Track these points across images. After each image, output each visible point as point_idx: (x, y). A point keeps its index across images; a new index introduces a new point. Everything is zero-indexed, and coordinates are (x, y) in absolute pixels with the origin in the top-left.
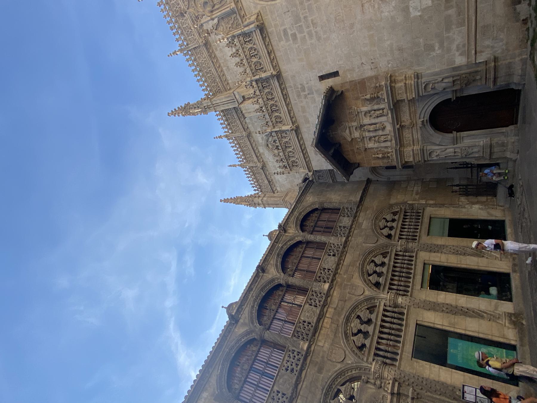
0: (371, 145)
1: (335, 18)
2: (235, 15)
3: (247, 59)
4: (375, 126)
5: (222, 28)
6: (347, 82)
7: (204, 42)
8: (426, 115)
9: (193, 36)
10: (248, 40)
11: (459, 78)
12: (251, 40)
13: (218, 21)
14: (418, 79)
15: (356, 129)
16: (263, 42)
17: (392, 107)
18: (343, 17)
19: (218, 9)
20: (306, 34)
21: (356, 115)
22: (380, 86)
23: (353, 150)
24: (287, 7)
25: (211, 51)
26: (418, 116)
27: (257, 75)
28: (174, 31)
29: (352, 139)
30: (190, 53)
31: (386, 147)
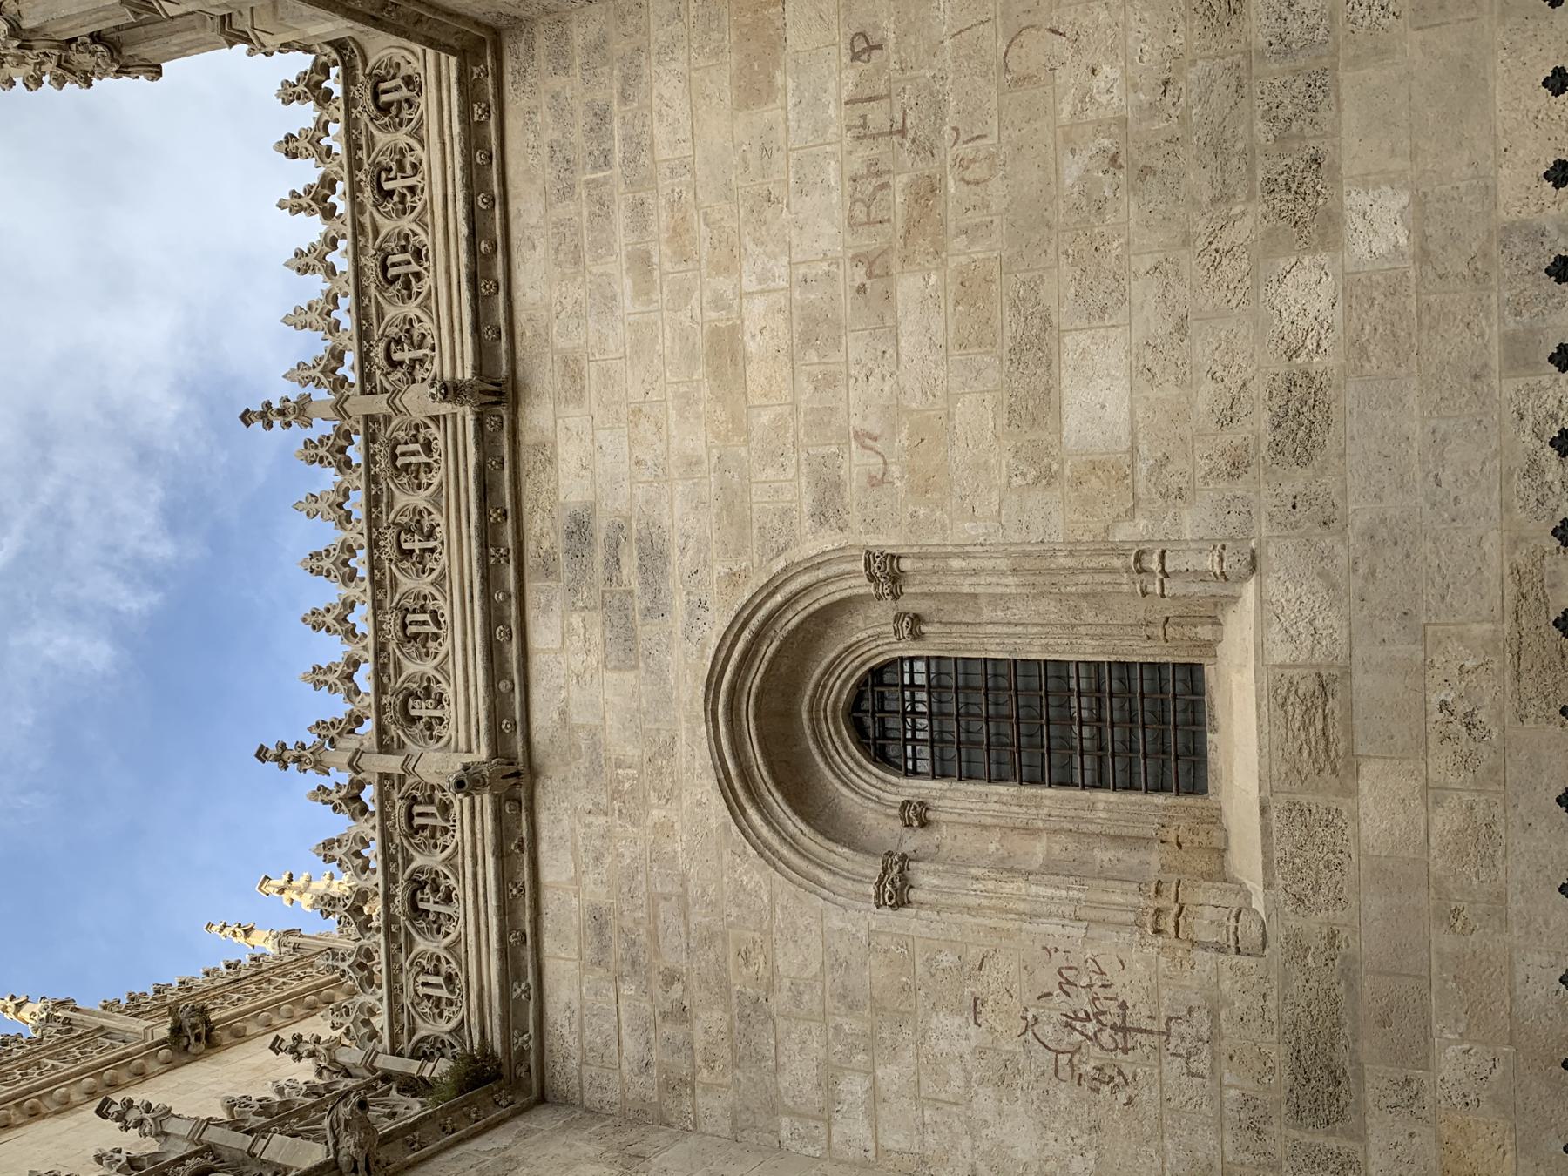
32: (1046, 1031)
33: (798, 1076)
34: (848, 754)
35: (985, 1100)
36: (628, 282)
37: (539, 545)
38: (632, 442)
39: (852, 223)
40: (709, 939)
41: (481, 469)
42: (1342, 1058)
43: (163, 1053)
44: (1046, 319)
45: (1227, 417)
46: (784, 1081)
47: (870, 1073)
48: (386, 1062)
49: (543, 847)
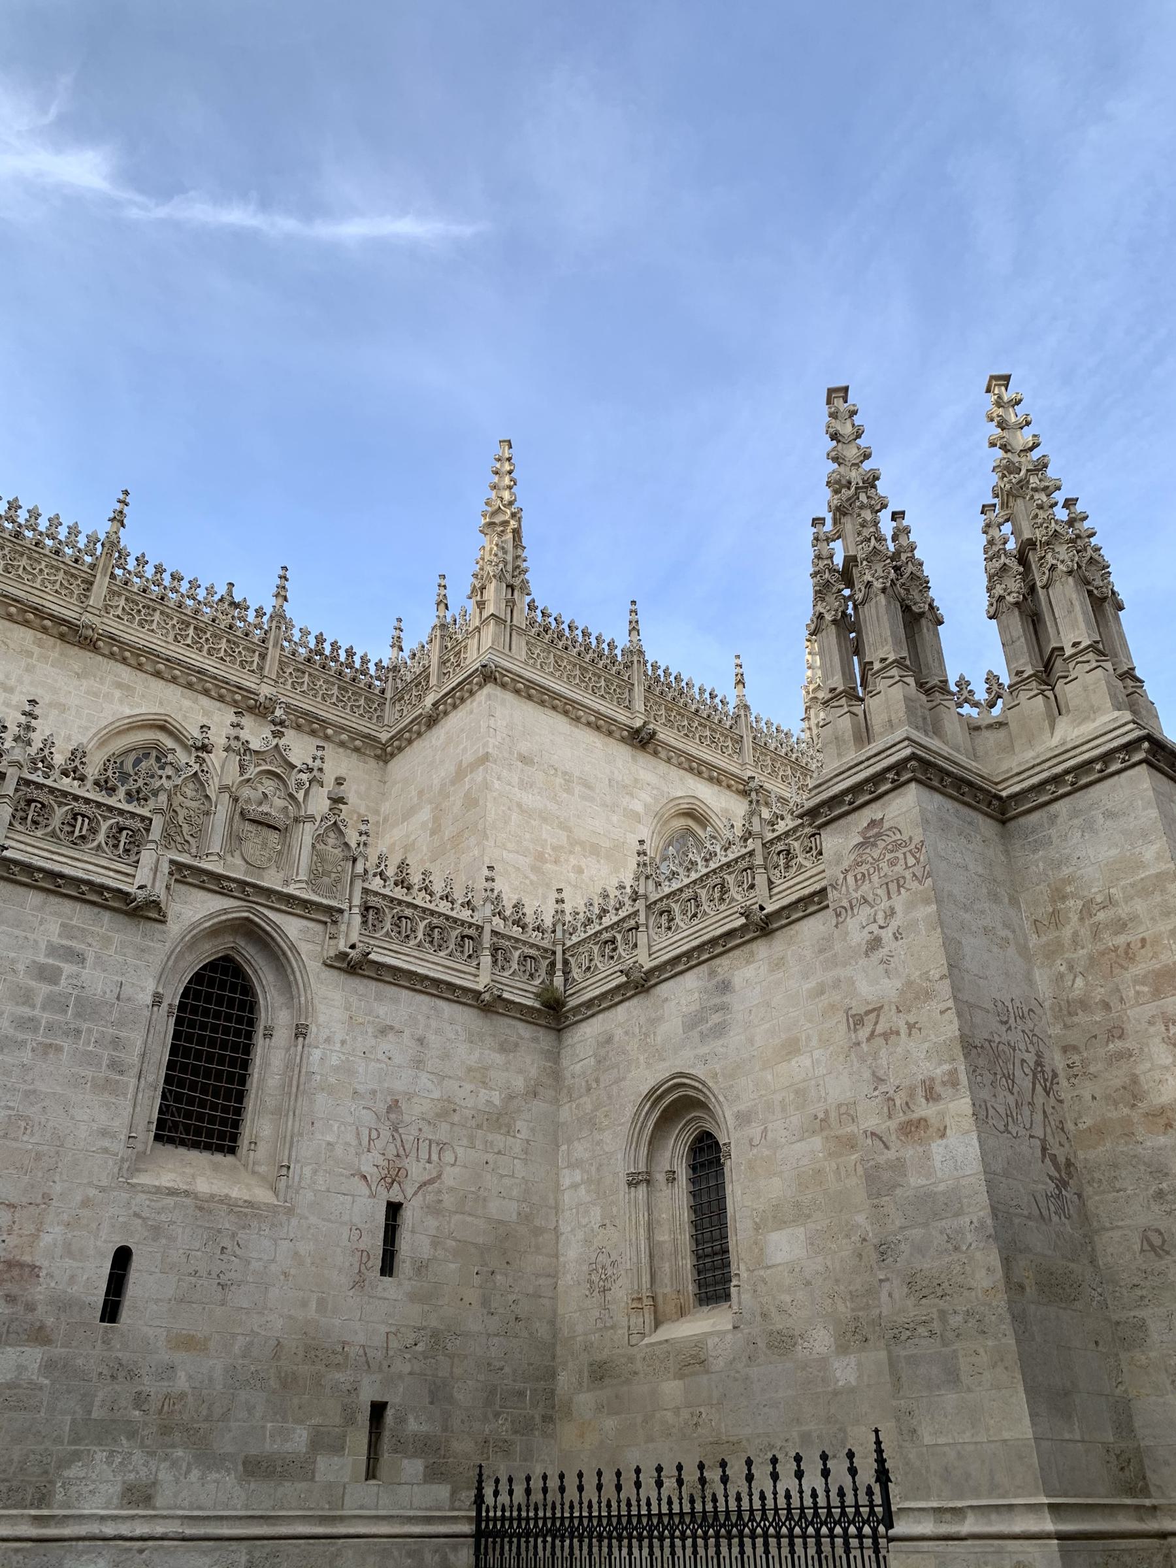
1: (27, 1119)
2: (194, 851)
3: (76, 798)
5: (189, 793)
7: (90, 632)
9: (119, 612)
10: (123, 840)
12: (116, 846)
13: (207, 796)
16: (98, 880)
18: (15, 1139)
19: (232, 819)
20: (36, 1012)
24: (129, 999)
25: (48, 623)
27: (16, 790)
28: (167, 580)
30: (88, 559)
32: (600, 1259)
33: (580, 1150)
34: (688, 1137)
35: (580, 1235)
36: (813, 984)
37: (719, 965)
38: (757, 1005)
39: (839, 1106)
40: (610, 1097)
41: (734, 930)
42: (607, 1381)
43: (625, 733)
44: (809, 1216)
45: (781, 1310)
46: (576, 1143)
47: (583, 1182)
48: (559, 949)
49: (626, 1004)
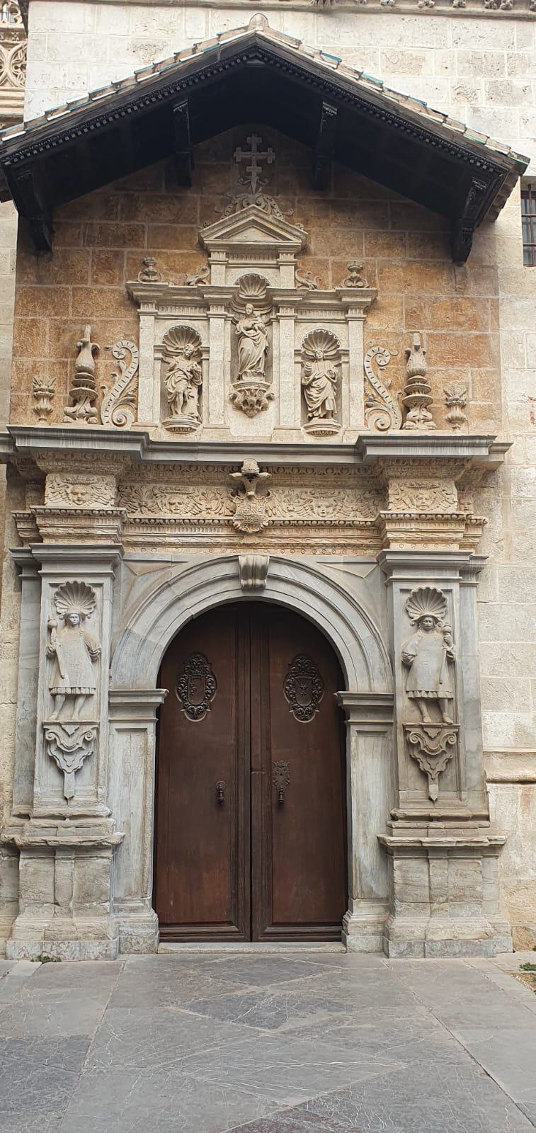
0: (153, 330)
4: (262, 371)
6: (496, 293)
8: (282, 587)
11: (449, 720)
14: (465, 571)
15: (255, 281)
17: (371, 451)
21: (337, 295)
22: (450, 421)
23: (132, 237)
26: (286, 554)
29: (205, 250)
31: (131, 400)
